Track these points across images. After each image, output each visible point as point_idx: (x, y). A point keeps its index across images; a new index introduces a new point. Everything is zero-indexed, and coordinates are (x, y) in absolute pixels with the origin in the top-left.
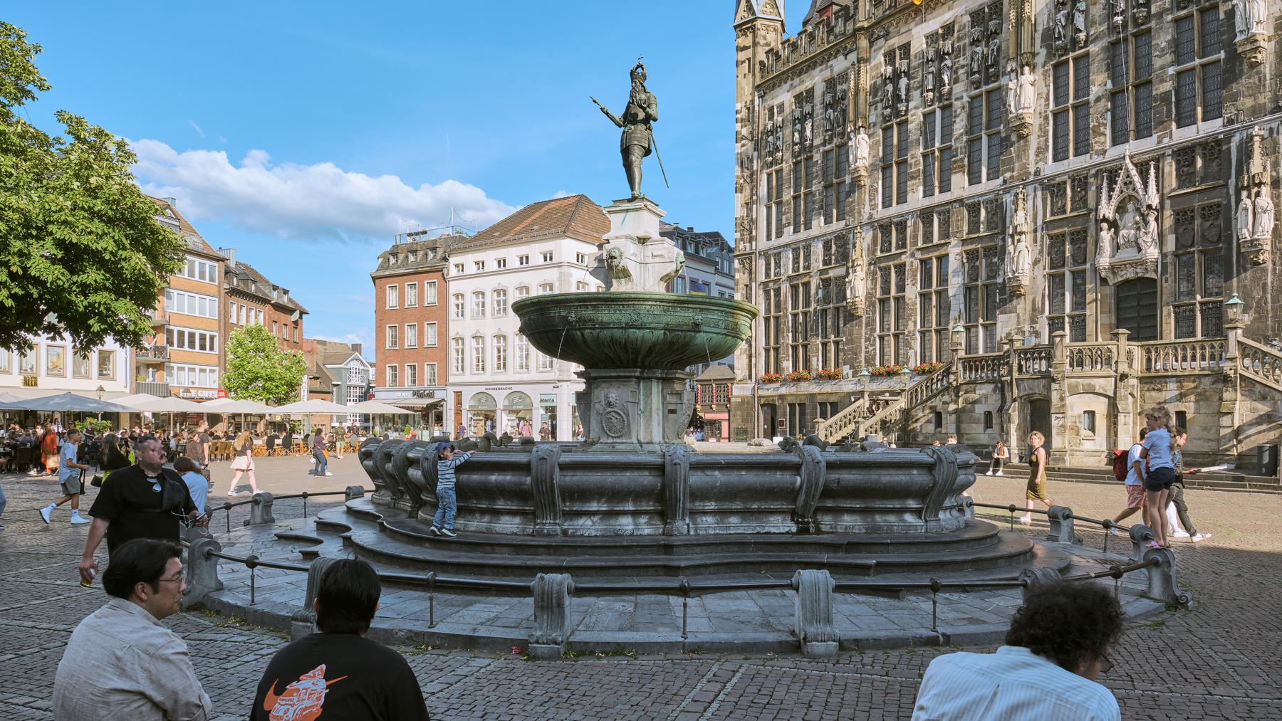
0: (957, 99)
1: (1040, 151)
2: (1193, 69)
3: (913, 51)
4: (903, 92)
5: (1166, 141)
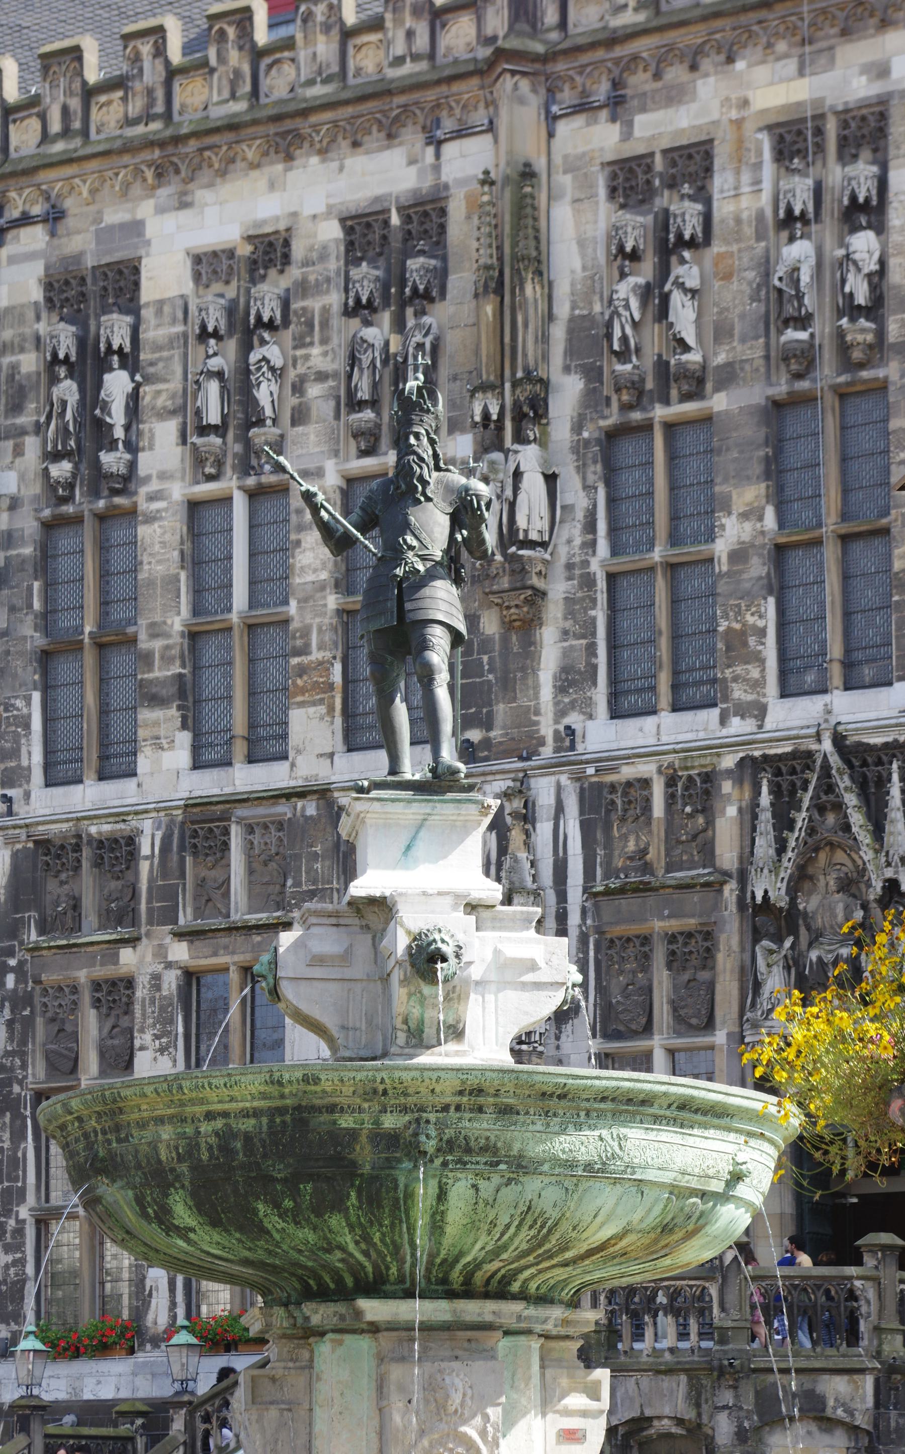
1: (572, 680)
3: (148, 293)
4: (117, 417)
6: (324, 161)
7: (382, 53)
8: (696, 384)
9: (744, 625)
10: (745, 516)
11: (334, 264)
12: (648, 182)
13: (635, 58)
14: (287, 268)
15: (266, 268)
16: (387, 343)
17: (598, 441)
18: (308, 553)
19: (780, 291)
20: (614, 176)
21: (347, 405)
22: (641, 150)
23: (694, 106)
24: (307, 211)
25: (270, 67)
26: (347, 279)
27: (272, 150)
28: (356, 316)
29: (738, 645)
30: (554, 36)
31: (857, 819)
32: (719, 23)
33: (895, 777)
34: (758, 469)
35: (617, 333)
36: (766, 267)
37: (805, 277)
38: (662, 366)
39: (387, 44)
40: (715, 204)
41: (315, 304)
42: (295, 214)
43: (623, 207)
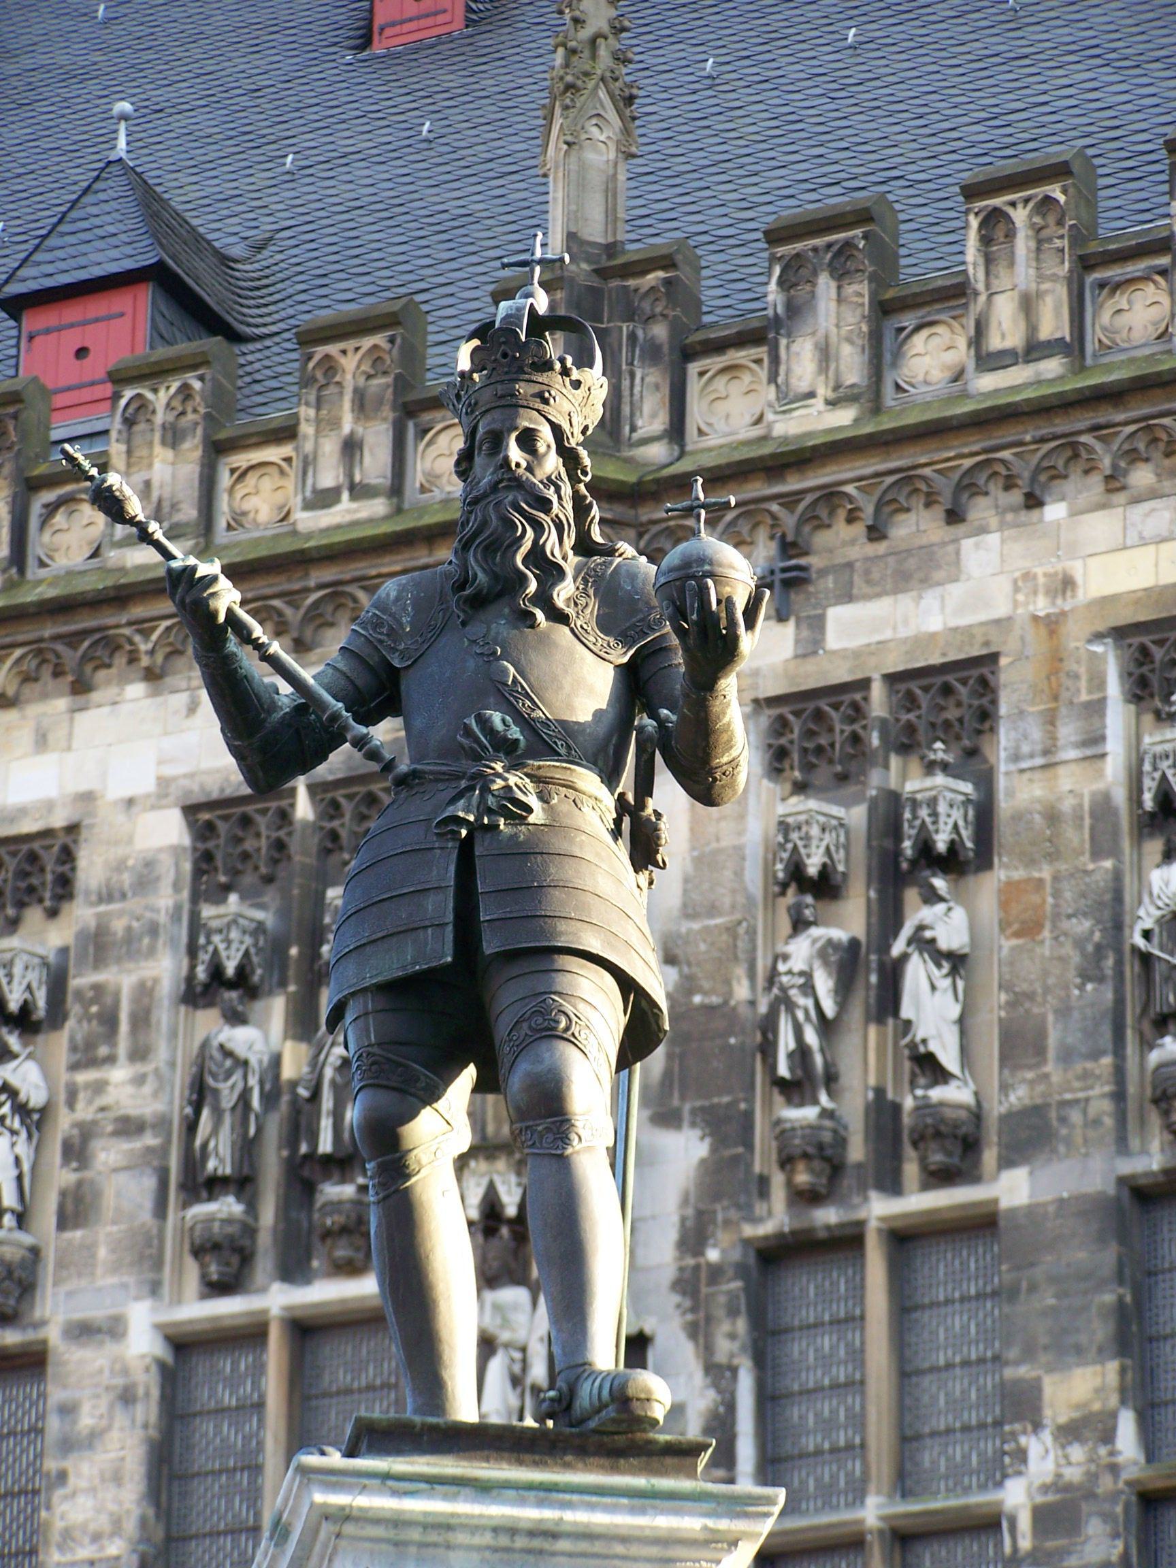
0: (83, 1331)
6: (155, 693)
7: (290, 484)
8: (957, 1148)
10: (1069, 1433)
11: (166, 899)
12: (855, 739)
13: (831, 496)
14: (66, 907)
15: (21, 905)
16: (276, 1061)
17: (741, 1270)
18: (81, 1499)
19: (1146, 959)
20: (781, 726)
21: (183, 1187)
22: (841, 674)
23: (955, 591)
24: (115, 790)
25: (52, 509)
26: (196, 925)
27: (47, 671)
28: (210, 1004)
30: (657, 452)
32: (1009, 433)
34: (1101, 1330)
35: (786, 1041)
36: (1113, 909)
38: (883, 1113)
39: (308, 463)
40: (1002, 783)
41: (122, 979)
42: (87, 798)
43: (800, 788)
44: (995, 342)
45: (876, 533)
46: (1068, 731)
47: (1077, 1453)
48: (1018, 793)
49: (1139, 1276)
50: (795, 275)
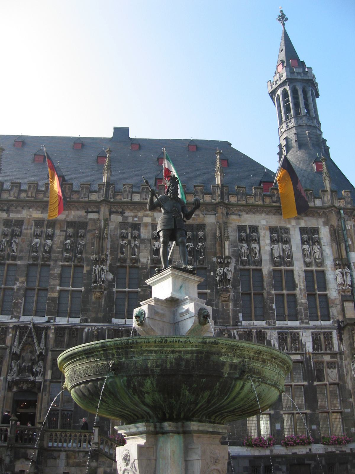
2: (68, 291)
5: (52, 321)
8: (14, 258)
9: (18, 301)
10: (20, 283)
12: (11, 224)
13: (13, 204)
19: (33, 246)
29: (16, 305)
31: (35, 340)
33: (44, 333)
36: (31, 242)
37: (38, 245)
38: (9, 254)
40: (23, 230)
44: (28, 195)
45: (16, 208)
46: (29, 227)
47: (21, 284)
48: (24, 231)
49: (28, 271)
50: (12, 186)
